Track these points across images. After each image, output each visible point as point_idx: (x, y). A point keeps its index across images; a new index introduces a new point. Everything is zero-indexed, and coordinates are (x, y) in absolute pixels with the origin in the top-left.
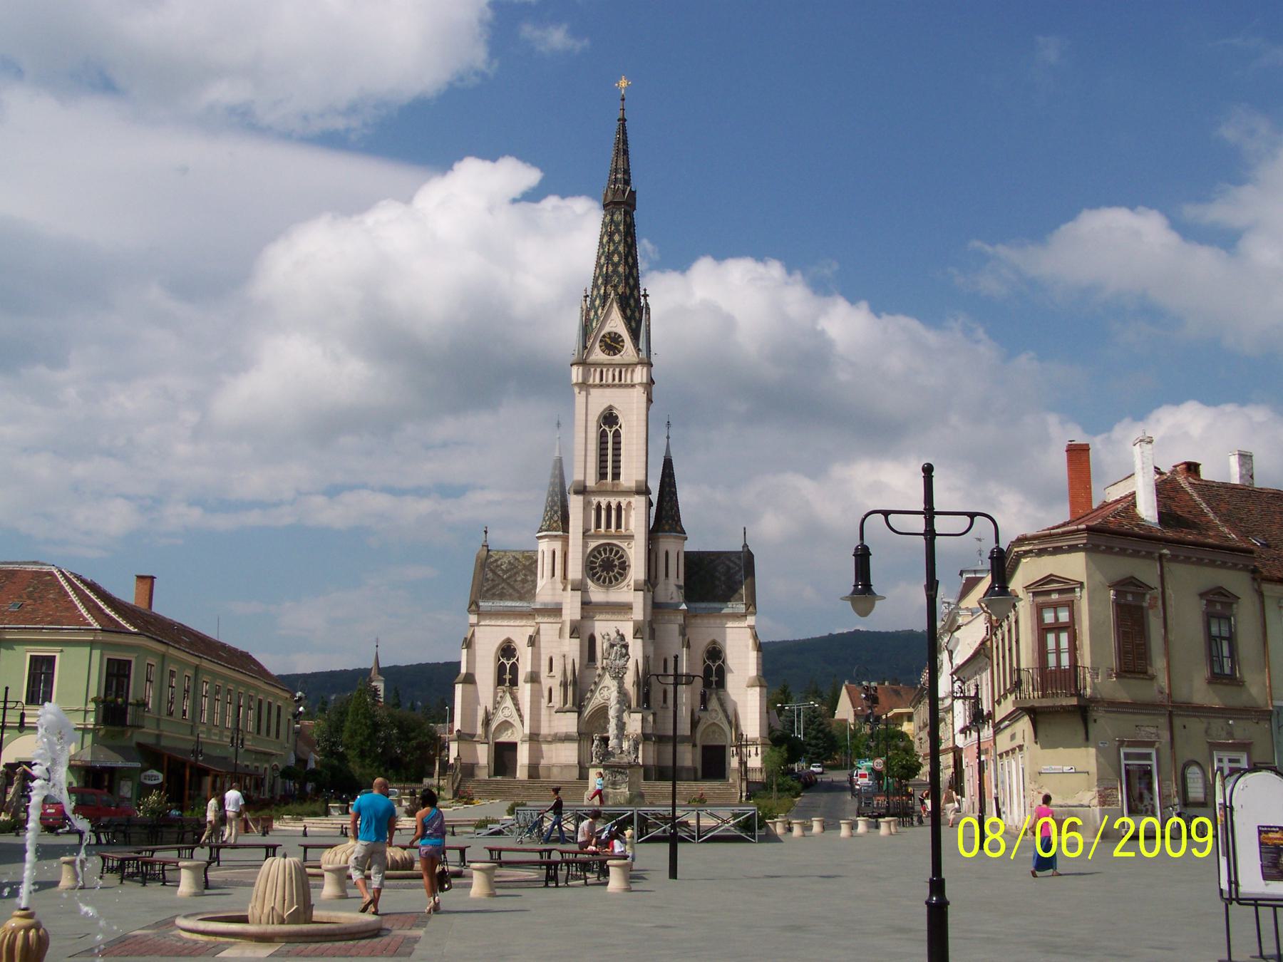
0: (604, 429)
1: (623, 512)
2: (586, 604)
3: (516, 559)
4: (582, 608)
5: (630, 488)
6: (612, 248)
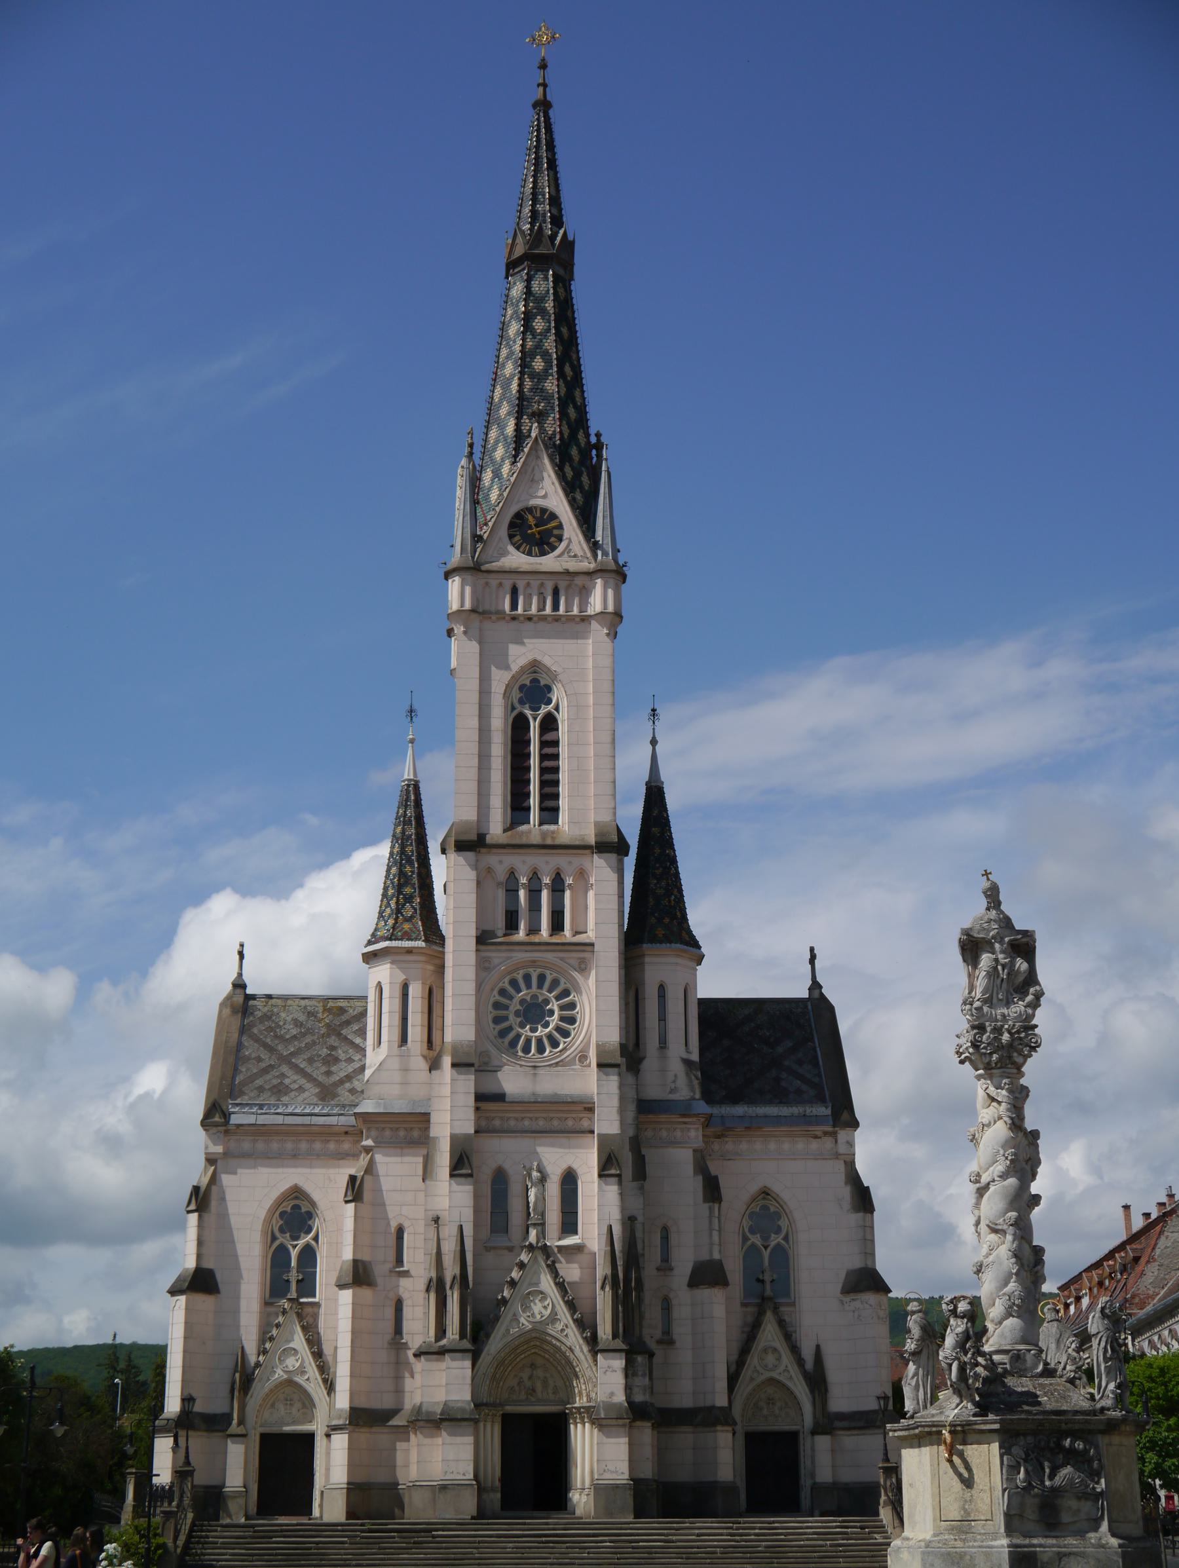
1: (568, 894)
2: (487, 1099)
4: (477, 1109)
6: (529, 344)
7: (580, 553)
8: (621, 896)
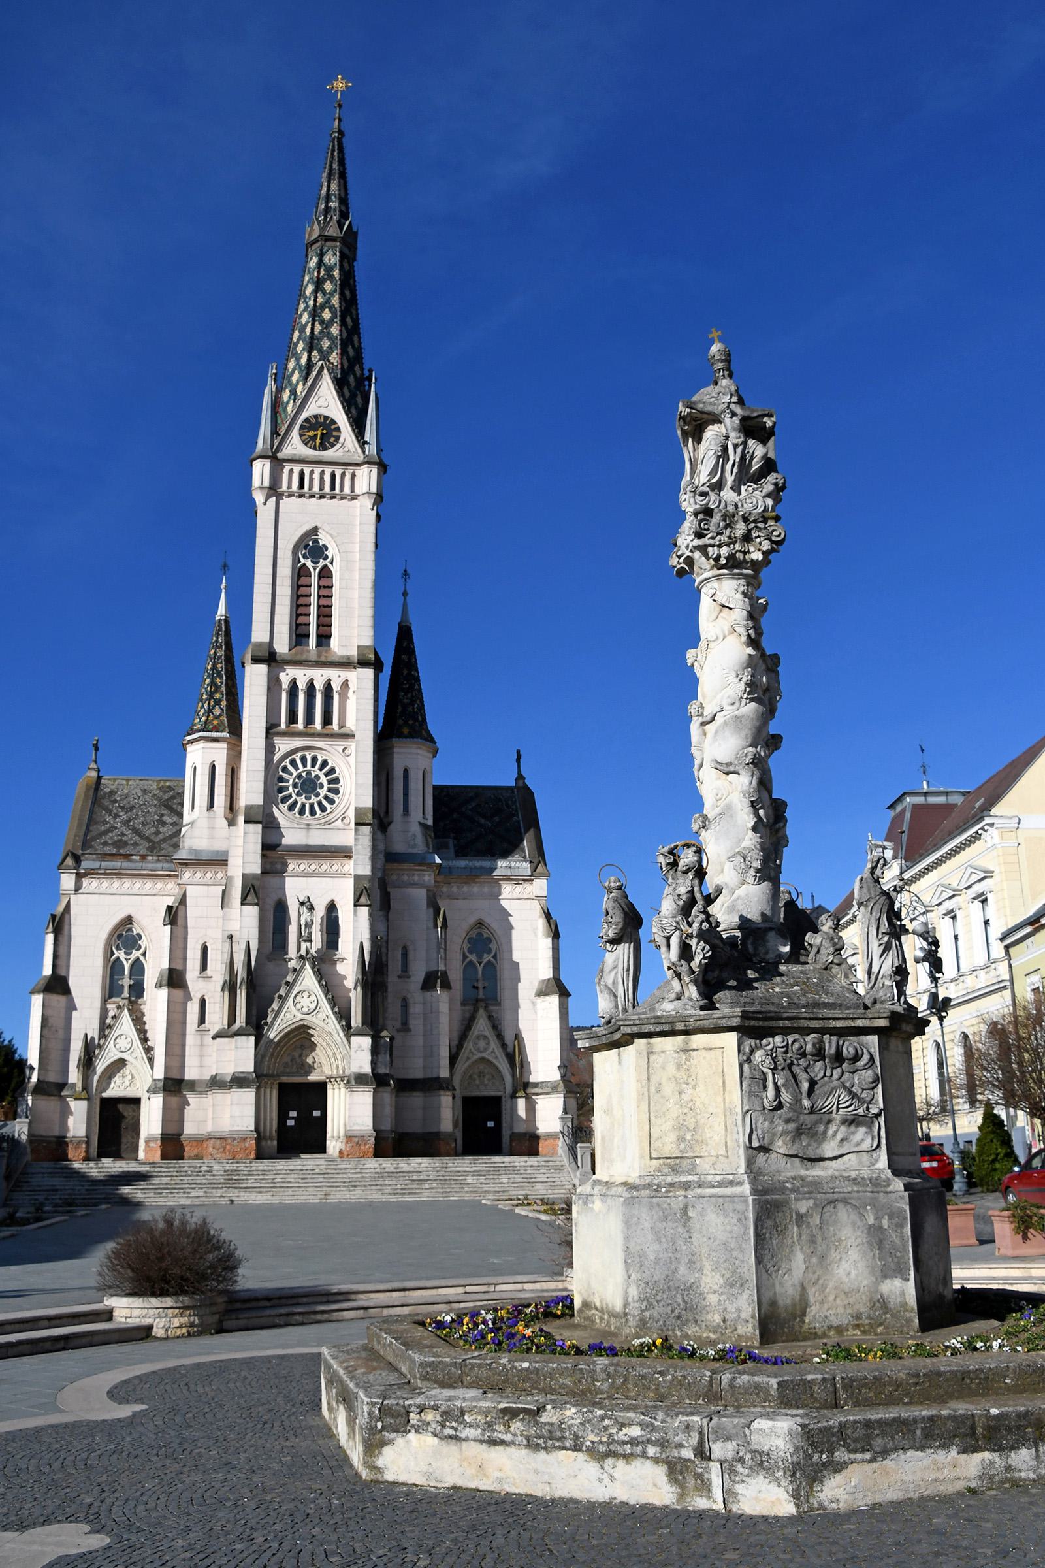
0: (304, 565)
3: (145, 791)
4: (263, 856)
5: (348, 657)
6: (320, 300)
7: (352, 450)
8: (376, 700)
